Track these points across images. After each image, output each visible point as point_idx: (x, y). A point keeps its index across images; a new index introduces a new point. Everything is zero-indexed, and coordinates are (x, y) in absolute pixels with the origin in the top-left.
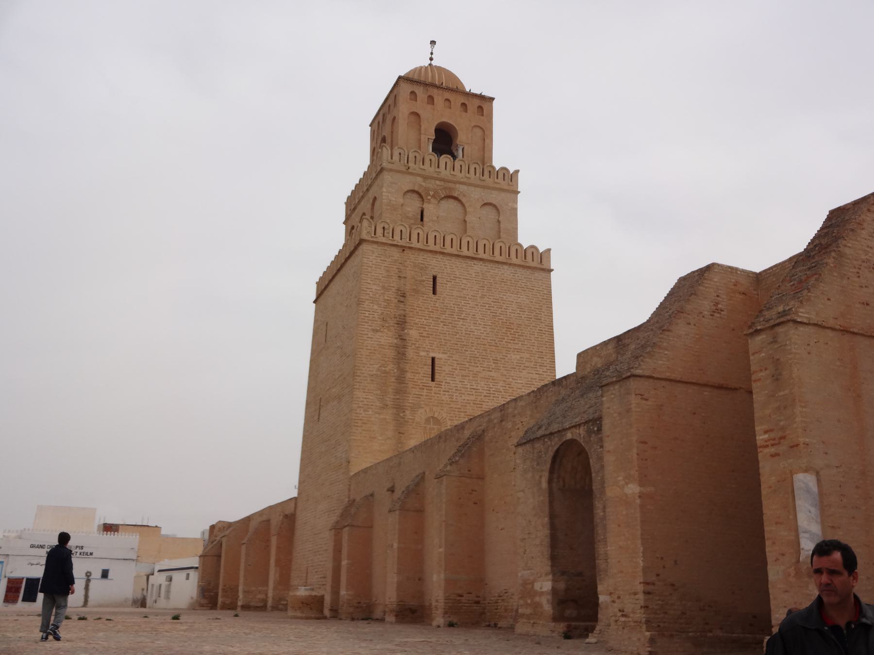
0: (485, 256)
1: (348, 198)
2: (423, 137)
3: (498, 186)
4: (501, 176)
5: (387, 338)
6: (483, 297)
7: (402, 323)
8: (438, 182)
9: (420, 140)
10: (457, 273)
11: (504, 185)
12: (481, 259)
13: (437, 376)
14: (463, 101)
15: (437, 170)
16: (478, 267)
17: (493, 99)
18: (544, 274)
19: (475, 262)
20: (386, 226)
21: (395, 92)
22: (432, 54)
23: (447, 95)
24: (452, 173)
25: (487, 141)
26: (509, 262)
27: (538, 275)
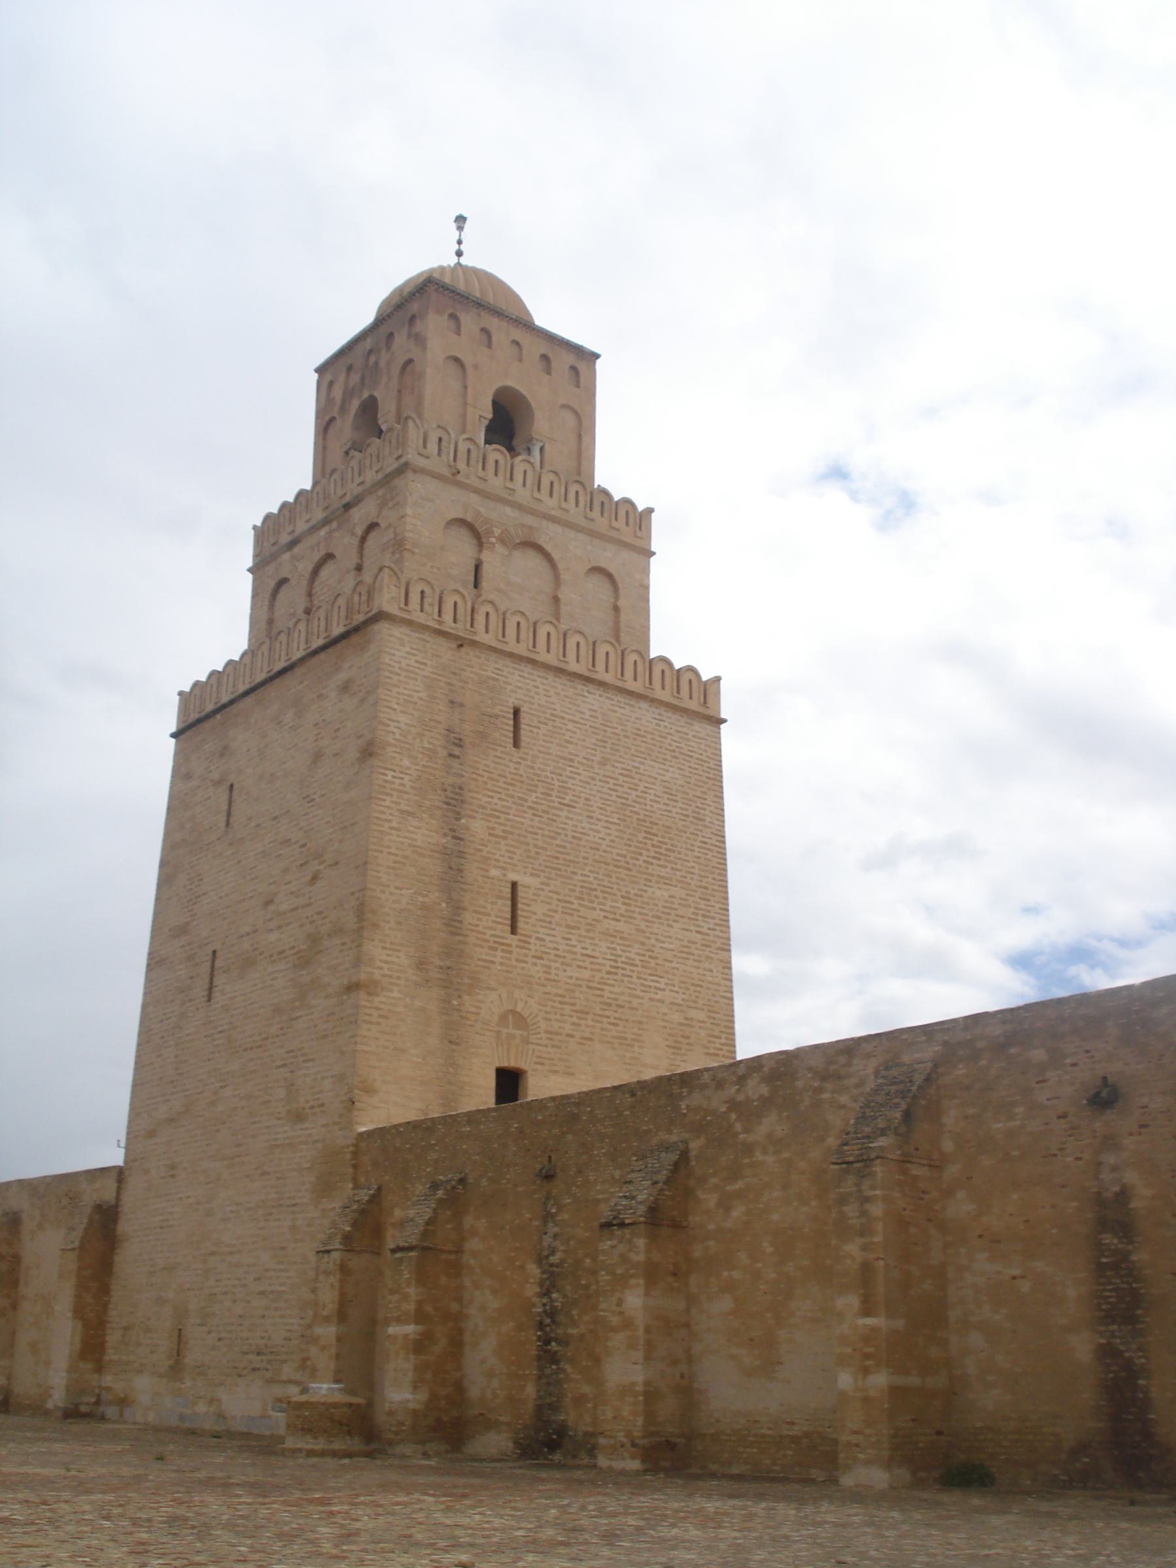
0: (608, 678)
1: (268, 517)
2: (470, 410)
3: (613, 534)
4: (622, 514)
5: (425, 833)
6: (604, 762)
7: (455, 803)
8: (508, 510)
9: (464, 416)
10: (557, 706)
11: (626, 535)
12: (602, 684)
13: (521, 924)
14: (543, 351)
15: (509, 485)
16: (595, 700)
17: (597, 356)
18: (710, 728)
19: (591, 687)
20: (428, 590)
21: (415, 307)
22: (460, 242)
23: (518, 334)
24: (536, 494)
25: (585, 439)
26: (649, 693)
27: (700, 728)
